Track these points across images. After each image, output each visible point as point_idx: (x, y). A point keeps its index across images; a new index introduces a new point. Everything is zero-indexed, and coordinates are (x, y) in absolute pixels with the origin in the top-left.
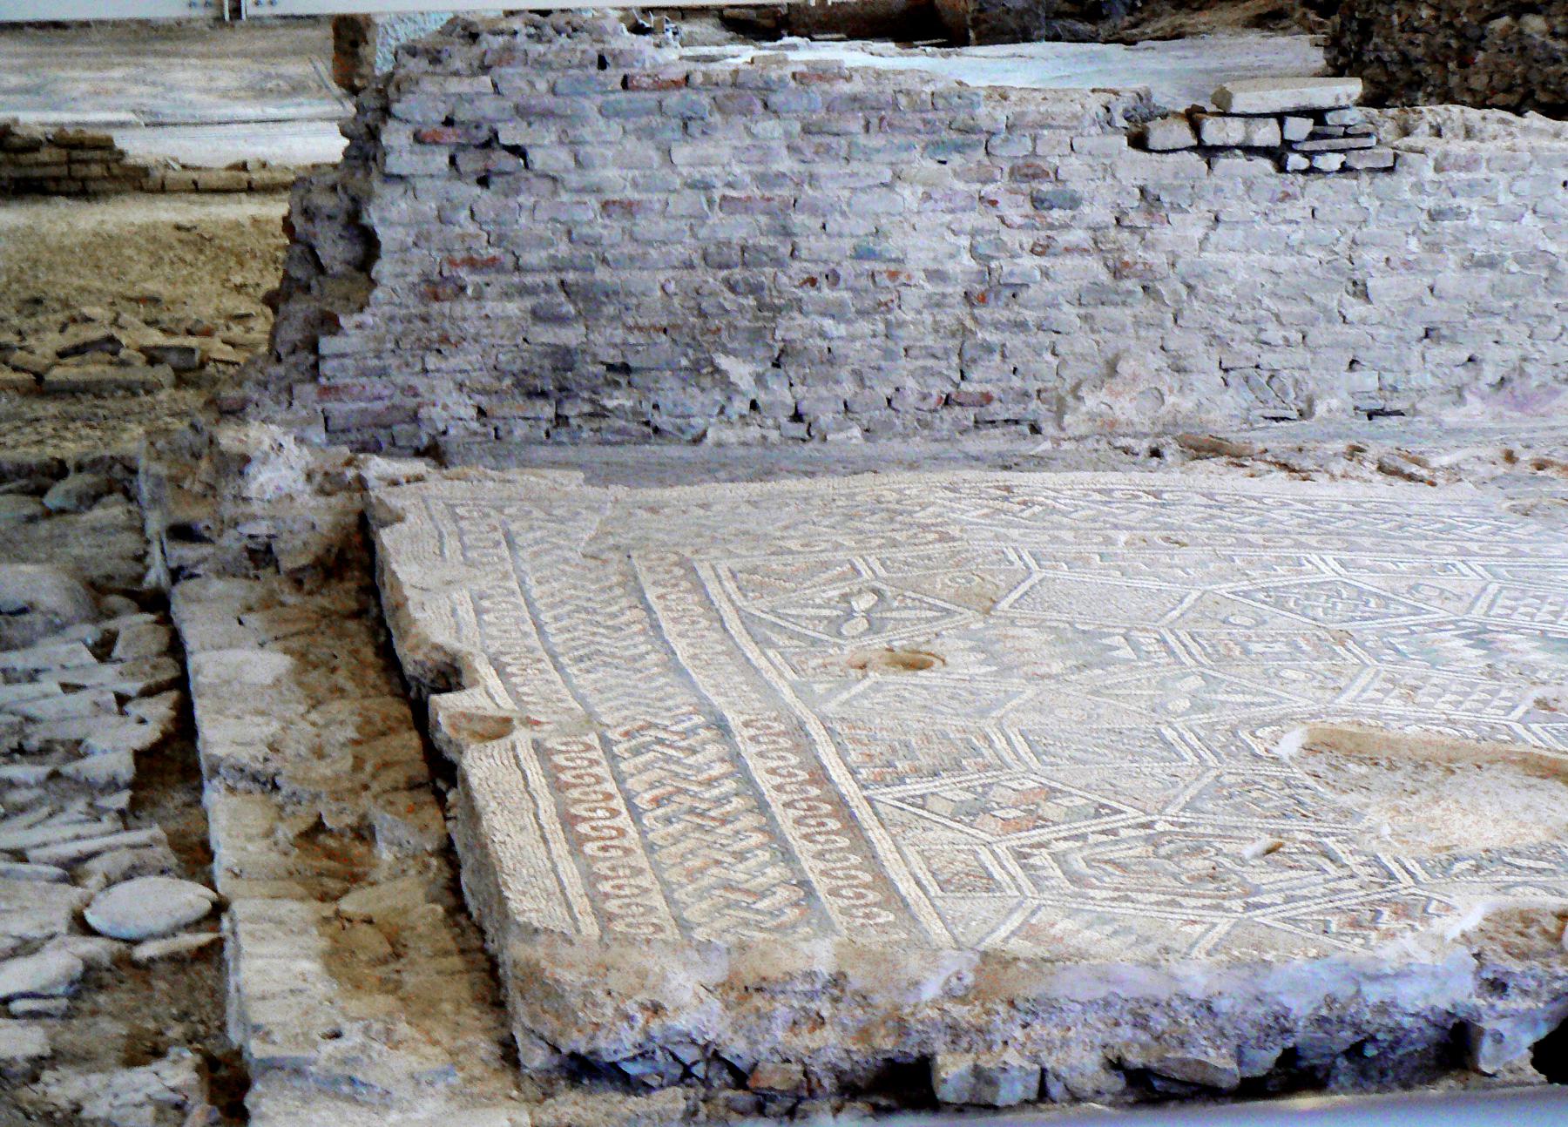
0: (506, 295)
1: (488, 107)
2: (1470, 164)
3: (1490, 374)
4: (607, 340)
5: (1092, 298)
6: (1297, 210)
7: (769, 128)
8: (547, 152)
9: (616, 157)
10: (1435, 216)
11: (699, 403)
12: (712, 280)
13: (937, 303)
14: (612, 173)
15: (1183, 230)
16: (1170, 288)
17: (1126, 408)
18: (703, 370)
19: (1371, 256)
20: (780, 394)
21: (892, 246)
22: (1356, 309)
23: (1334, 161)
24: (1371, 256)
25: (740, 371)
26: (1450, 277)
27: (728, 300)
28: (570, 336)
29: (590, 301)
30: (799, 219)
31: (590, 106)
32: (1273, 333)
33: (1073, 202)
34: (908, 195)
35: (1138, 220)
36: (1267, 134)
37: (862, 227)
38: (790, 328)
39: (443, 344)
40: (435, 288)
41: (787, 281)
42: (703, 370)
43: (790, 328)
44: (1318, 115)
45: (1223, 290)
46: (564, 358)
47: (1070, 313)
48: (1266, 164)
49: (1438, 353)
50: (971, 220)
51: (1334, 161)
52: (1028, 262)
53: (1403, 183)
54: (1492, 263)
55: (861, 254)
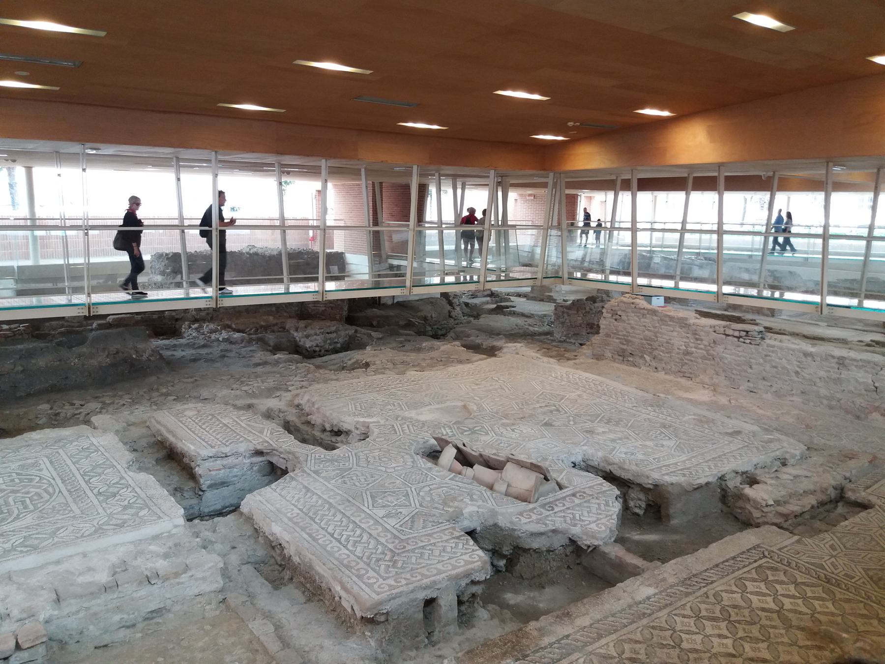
0: (617, 338)
1: (617, 308)
2: (773, 346)
3: (774, 389)
4: (629, 349)
5: (704, 358)
6: (740, 349)
7: (655, 318)
8: (624, 317)
9: (633, 319)
10: (766, 356)
11: (641, 361)
12: (645, 342)
13: (678, 354)
14: (632, 322)
15: (720, 349)
16: (717, 359)
17: (707, 380)
18: (642, 357)
19: (753, 361)
20: (654, 364)
21: (672, 342)
22: (750, 371)
23: (748, 341)
24: (753, 361)
25: (647, 358)
26: (768, 367)
27: (647, 346)
28: (625, 347)
29: (628, 342)
30: (658, 335)
31: (630, 310)
32: (734, 372)
33: (702, 340)
34: (675, 334)
35: (712, 345)
36: (737, 334)
37: (668, 338)
38: (656, 353)
39: (608, 345)
40: (608, 335)
41: (656, 344)
42: (642, 357)
43: (656, 353)
44: (747, 332)
45: (726, 362)
46: (624, 351)
47: (700, 360)
48: (736, 339)
49: (765, 383)
50: (685, 340)
51: (748, 341)
52: (693, 349)
53: (760, 348)
54: (776, 367)
55: (667, 343)
